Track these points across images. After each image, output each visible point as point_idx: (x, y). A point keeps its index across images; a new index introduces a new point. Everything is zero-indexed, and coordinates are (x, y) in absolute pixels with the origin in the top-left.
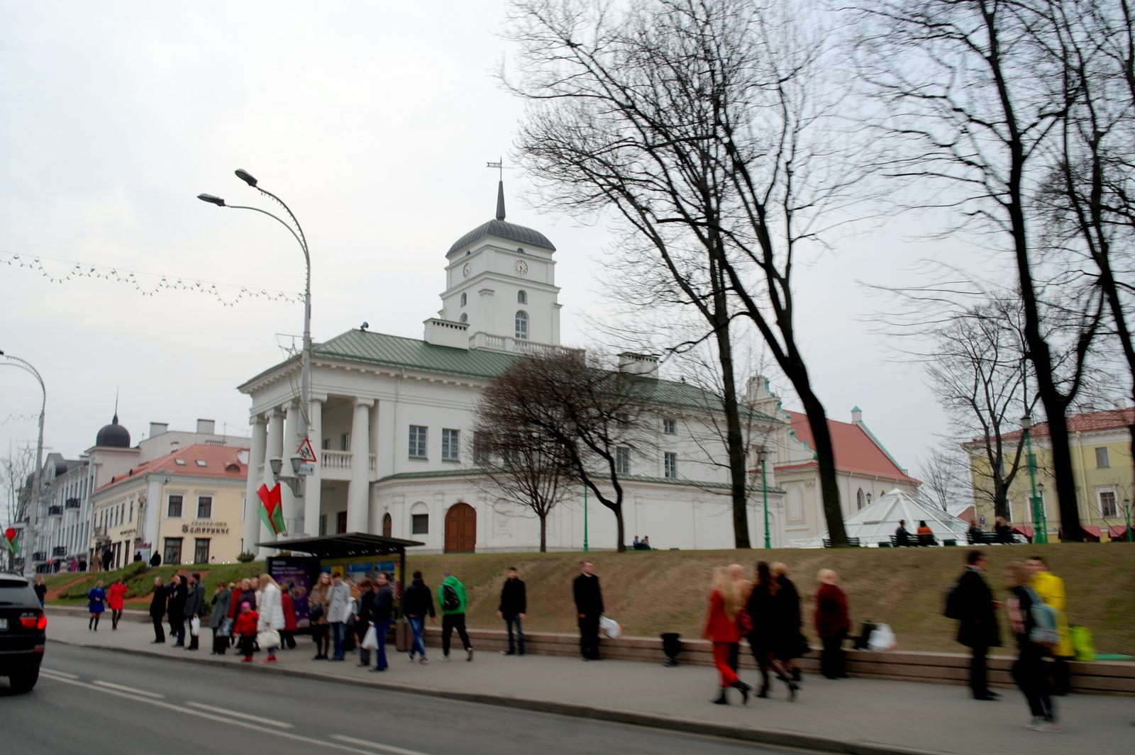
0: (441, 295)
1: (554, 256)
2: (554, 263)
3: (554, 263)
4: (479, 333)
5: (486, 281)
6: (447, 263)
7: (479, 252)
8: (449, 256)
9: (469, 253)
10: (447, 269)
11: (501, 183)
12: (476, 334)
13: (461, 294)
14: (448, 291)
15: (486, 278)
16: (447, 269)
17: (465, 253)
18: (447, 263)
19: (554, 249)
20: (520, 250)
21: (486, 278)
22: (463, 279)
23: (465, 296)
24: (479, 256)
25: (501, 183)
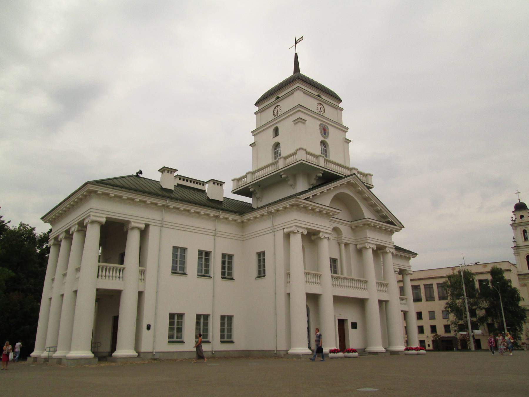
0: (252, 132)
1: (341, 105)
2: (342, 109)
3: (342, 109)
4: (301, 149)
5: (299, 113)
6: (256, 109)
7: (291, 93)
8: (256, 104)
9: (278, 98)
10: (256, 113)
11: (296, 55)
12: (297, 150)
13: (271, 131)
14: (257, 129)
15: (299, 111)
16: (256, 113)
17: (274, 99)
18: (256, 109)
19: (340, 101)
21: (299, 111)
22: (273, 117)
23: (276, 130)
24: (292, 96)
25: (296, 55)
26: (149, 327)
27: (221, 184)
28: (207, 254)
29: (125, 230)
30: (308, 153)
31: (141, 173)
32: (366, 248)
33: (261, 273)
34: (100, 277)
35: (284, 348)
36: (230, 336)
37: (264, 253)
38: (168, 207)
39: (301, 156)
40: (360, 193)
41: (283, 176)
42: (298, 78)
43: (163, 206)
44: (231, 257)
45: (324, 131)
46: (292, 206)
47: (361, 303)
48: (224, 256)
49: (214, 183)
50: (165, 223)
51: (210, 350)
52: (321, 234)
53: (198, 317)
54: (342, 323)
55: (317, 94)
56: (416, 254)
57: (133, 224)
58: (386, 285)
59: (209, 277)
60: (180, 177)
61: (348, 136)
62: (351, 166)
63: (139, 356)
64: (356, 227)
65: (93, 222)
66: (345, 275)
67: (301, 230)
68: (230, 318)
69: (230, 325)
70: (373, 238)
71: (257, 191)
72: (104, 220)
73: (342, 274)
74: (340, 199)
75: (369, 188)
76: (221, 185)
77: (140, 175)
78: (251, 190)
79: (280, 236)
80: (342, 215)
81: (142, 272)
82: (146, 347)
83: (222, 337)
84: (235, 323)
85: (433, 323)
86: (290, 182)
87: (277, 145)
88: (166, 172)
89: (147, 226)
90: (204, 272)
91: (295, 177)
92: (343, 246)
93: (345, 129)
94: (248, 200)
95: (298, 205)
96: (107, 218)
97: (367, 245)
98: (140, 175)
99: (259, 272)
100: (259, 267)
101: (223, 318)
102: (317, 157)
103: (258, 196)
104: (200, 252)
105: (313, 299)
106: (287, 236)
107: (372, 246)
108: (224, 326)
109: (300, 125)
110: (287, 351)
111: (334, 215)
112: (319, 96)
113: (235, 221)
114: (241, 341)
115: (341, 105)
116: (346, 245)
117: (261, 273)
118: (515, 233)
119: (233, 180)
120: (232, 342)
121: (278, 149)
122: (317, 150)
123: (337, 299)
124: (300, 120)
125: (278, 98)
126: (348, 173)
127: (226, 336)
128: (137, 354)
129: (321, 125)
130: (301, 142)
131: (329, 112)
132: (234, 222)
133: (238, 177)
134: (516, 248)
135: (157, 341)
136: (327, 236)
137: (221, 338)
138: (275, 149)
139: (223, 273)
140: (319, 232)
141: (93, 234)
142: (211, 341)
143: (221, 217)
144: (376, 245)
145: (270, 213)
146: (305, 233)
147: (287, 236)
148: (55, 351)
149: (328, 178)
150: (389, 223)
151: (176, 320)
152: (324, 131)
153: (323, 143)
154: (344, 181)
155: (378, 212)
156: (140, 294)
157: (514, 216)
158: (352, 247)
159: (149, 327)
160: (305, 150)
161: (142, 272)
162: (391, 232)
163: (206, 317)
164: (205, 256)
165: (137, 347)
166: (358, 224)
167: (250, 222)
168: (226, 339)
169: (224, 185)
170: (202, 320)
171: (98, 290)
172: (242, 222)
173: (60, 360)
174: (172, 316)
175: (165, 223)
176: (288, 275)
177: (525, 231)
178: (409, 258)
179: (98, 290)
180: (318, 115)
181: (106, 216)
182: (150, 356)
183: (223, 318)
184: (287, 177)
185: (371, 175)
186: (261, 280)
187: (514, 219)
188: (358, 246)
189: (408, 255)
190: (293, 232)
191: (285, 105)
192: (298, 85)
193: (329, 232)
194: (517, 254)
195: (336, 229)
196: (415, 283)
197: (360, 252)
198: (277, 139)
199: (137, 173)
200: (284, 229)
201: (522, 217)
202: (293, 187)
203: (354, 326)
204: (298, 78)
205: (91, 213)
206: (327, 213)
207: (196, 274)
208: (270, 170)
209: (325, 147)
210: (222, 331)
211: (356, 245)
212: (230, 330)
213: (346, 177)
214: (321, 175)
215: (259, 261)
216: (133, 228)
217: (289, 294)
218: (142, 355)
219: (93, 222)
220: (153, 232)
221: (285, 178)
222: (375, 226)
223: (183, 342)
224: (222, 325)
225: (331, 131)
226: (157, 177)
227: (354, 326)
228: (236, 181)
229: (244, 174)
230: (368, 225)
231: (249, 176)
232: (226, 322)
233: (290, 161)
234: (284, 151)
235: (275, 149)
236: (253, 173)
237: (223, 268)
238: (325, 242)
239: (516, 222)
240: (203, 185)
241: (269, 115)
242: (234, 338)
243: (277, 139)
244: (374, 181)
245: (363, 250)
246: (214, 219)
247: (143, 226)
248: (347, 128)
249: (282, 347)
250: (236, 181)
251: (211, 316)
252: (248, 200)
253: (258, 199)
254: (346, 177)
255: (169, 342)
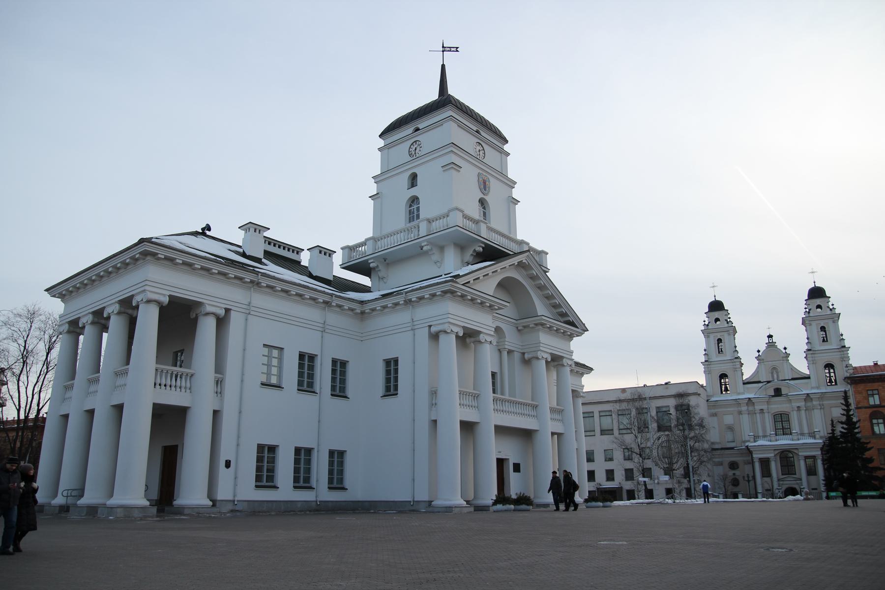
1: (506, 147)
2: (508, 154)
3: (508, 154)
5: (452, 155)
6: (381, 143)
9: (417, 129)
10: (380, 149)
11: (443, 66)
12: (449, 211)
13: (405, 178)
16: (380, 149)
17: (411, 130)
18: (381, 143)
19: (507, 142)
20: (477, 132)
23: (413, 180)
25: (443, 66)
26: (228, 464)
27: (329, 253)
28: (312, 358)
29: (193, 316)
30: (466, 217)
31: (209, 229)
32: (537, 358)
33: (391, 388)
34: (158, 386)
35: (426, 499)
36: (341, 480)
37: (396, 361)
38: (258, 284)
39: (457, 219)
40: (533, 278)
41: (425, 248)
42: (445, 100)
43: (252, 282)
44: (344, 364)
45: (484, 186)
46: (445, 292)
47: (527, 435)
48: (334, 362)
49: (320, 252)
50: (253, 309)
51: (314, 499)
52: (481, 335)
53: (298, 451)
54: (501, 462)
55: (475, 129)
56: (592, 369)
57: (209, 309)
58: (560, 412)
59: (314, 392)
60: (269, 241)
61: (516, 193)
62: (520, 237)
63: (214, 505)
64: (524, 327)
65: (149, 301)
66: (507, 397)
67: (456, 329)
68: (341, 454)
69: (341, 464)
70: (548, 343)
71: (380, 267)
72: (165, 300)
73: (502, 394)
74: (505, 285)
75: (545, 272)
76: (330, 255)
77: (208, 233)
78: (372, 265)
79: (423, 335)
80: (509, 310)
81: (219, 382)
82: (224, 493)
83: (331, 481)
84: (348, 460)
85: (610, 466)
86: (436, 257)
87: (414, 200)
88: (252, 230)
89: (227, 311)
90: (306, 383)
91: (442, 249)
92: (505, 353)
93: (511, 184)
94: (364, 280)
95: (452, 292)
96: (170, 296)
97: (540, 354)
98: (208, 233)
99: (388, 389)
100: (388, 380)
101: (332, 453)
102: (477, 222)
103: (381, 274)
104: (302, 356)
105: (468, 427)
106: (435, 337)
107: (545, 355)
108: (299, 464)
109: (453, 172)
110: (430, 503)
111: (499, 309)
112: (477, 132)
113: (352, 310)
114: (358, 486)
115: (506, 147)
116: (510, 352)
117: (391, 388)
118: (707, 343)
119: (342, 249)
120: (344, 489)
121: (415, 207)
122: (475, 211)
123: (500, 430)
124: (453, 166)
125: (417, 129)
126: (516, 248)
127: (336, 481)
128: (211, 503)
129: (479, 174)
130: (451, 197)
131: (491, 157)
132: (350, 313)
133: (351, 243)
134: (707, 363)
135: (239, 486)
136: (489, 339)
137: (294, 482)
138: (411, 206)
139: (333, 388)
140: (479, 332)
141: (149, 322)
142: (314, 486)
143: (334, 304)
144: (551, 354)
145: (408, 302)
146: (461, 334)
147: (435, 337)
148: (82, 496)
149: (491, 254)
150: (570, 324)
151: (267, 454)
152: (484, 186)
153: (482, 202)
154: (515, 260)
155: (556, 306)
156: (216, 413)
157: (706, 319)
158: (517, 356)
159: (228, 464)
160: (462, 211)
161: (219, 382)
162: (571, 337)
163: (309, 451)
164: (307, 361)
165: (211, 495)
166: (526, 323)
167: (374, 313)
168: (301, 484)
169: (334, 256)
170: (303, 455)
171: (154, 404)
172: (363, 313)
173: (92, 510)
174: (261, 448)
175: (253, 309)
176: (434, 393)
177: (719, 341)
178: (582, 374)
179: (154, 404)
180: (478, 159)
181: (168, 293)
182: (230, 507)
183: (332, 453)
184: (431, 249)
185: (547, 254)
186: (390, 400)
187: (707, 323)
188: (526, 356)
189: (581, 370)
190: (445, 332)
191: (430, 140)
192: (450, 113)
193: (492, 333)
194: (707, 372)
195: (498, 330)
196: (589, 408)
197: (527, 362)
198: (414, 192)
199: (203, 229)
200: (430, 326)
201: (717, 320)
202: (438, 264)
203: (517, 468)
204: (445, 100)
205: (147, 288)
206: (491, 306)
207: (296, 387)
208: (401, 238)
209: (484, 208)
210: (331, 472)
211: (523, 354)
212: (341, 472)
213: (516, 254)
214: (481, 249)
215: (388, 372)
216: (207, 314)
217: (435, 421)
218: (218, 504)
219: (149, 301)
220: (236, 321)
221: (426, 252)
222: (550, 328)
223: (276, 487)
224: (331, 463)
225: (493, 184)
226: (238, 237)
227: (517, 468)
228: (347, 250)
229: (362, 239)
230: (542, 325)
231: (370, 243)
232: (336, 459)
233: (436, 226)
234: (425, 212)
235: (411, 206)
236: (374, 239)
237: (333, 379)
238: (487, 347)
239: (710, 327)
240: (298, 253)
241: (401, 153)
242: (347, 483)
243: (414, 192)
244: (551, 262)
245: (534, 362)
246: (323, 305)
247: (222, 312)
248: (515, 183)
249: (422, 495)
250: (347, 250)
251: (316, 450)
252: (364, 280)
253: (381, 279)
254: (516, 254)
255: (257, 486)
